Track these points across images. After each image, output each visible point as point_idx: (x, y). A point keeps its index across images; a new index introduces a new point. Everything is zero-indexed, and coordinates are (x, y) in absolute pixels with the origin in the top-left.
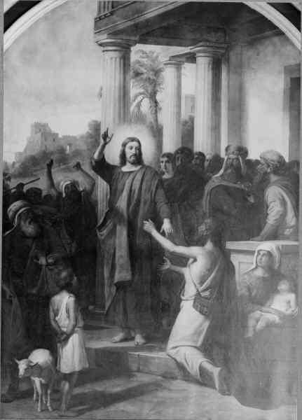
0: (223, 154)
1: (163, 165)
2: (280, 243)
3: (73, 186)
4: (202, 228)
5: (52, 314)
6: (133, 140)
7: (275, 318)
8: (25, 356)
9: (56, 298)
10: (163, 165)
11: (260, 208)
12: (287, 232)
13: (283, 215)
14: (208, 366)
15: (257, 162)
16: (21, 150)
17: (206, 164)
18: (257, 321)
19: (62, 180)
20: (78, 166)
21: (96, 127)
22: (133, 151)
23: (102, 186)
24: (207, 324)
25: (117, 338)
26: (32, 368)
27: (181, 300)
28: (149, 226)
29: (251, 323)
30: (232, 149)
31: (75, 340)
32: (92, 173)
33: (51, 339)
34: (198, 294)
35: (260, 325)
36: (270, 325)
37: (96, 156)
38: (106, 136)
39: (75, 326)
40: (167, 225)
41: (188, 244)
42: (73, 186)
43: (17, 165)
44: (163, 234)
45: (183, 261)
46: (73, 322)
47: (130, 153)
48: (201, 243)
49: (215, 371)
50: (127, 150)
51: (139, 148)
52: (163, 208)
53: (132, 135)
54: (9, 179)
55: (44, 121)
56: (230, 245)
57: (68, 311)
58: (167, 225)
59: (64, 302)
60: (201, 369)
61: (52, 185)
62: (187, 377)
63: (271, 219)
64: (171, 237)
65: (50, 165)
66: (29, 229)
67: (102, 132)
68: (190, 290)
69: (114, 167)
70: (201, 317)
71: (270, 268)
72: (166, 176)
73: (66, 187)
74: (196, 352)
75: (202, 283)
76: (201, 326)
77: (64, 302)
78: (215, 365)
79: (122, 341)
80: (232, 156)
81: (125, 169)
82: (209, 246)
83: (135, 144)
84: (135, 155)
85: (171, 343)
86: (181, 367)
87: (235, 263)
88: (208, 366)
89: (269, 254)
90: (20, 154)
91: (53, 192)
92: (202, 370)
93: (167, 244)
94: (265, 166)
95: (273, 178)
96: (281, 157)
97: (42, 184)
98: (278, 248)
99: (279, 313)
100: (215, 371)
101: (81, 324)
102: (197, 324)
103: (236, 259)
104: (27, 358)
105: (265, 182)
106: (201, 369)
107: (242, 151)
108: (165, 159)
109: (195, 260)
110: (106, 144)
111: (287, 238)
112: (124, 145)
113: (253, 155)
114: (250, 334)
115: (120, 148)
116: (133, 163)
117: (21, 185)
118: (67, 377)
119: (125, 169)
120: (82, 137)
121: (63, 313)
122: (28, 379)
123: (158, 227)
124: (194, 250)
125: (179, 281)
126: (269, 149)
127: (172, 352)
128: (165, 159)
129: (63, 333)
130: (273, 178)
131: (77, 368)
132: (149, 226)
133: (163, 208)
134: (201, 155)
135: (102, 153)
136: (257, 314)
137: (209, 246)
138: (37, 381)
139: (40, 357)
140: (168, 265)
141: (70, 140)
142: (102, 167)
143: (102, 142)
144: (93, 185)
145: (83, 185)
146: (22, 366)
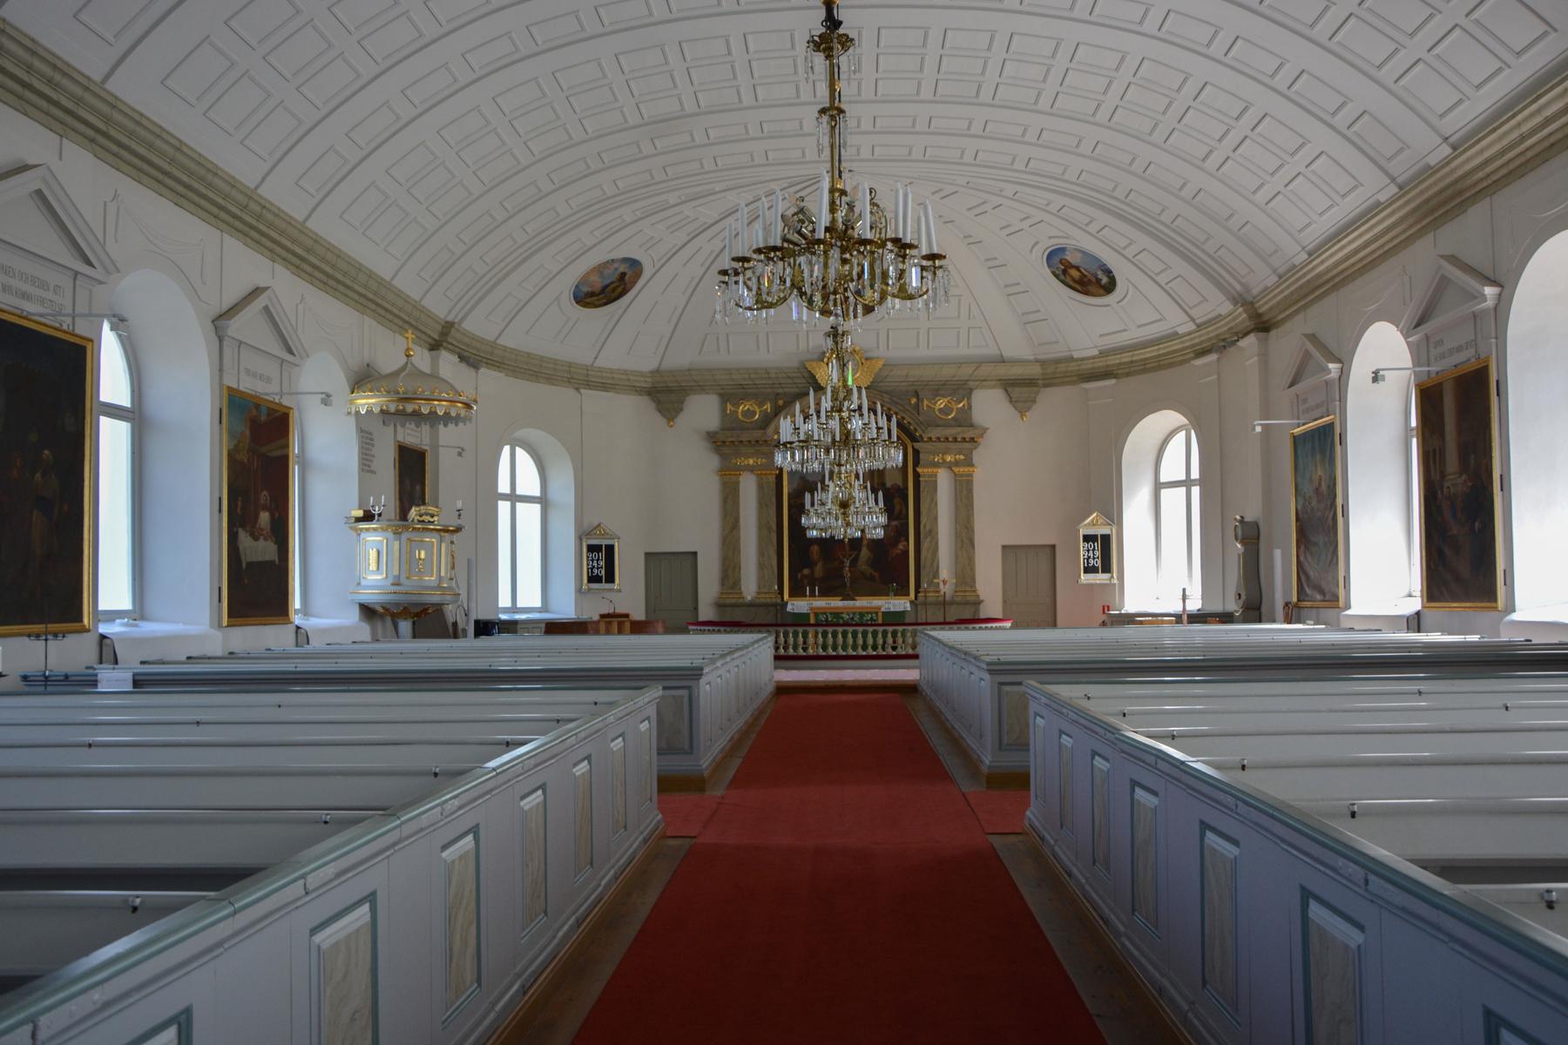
33: (811, 565)
139: (806, 571)
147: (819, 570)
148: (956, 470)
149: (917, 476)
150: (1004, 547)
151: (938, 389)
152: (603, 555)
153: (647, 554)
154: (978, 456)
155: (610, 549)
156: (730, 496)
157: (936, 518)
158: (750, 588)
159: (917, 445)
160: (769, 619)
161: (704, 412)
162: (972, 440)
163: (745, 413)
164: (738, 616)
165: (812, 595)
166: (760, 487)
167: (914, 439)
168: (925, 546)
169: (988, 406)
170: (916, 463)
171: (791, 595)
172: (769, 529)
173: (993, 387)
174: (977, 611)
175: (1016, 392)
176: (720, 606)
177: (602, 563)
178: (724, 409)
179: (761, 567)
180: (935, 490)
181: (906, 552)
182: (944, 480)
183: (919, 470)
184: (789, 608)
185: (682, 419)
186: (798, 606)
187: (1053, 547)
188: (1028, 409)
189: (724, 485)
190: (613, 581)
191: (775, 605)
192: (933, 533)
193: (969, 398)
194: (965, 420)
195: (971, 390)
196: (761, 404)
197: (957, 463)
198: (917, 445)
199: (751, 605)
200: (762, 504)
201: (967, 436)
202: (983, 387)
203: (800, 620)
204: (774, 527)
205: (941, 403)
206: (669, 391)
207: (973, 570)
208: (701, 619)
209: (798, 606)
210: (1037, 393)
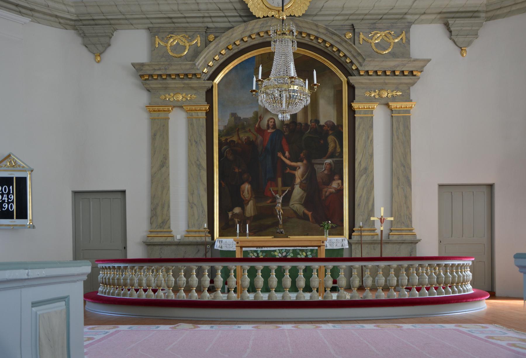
0: (309, 123)
1: (284, 129)
2: (335, 159)
3: (248, 138)
4: (302, 155)
5: (241, 193)
6: (272, 118)
7: (333, 190)
8: (231, 209)
9: (243, 186)
10: (284, 129)
11: (326, 145)
12: (337, 155)
13: (336, 147)
14: (306, 212)
15: (323, 126)
16: (226, 124)
17: (303, 127)
18: (326, 192)
19: (244, 136)
20: (250, 130)
21: (256, 113)
22: (272, 123)
23: (260, 138)
24: (305, 195)
25: (269, 202)
26: (234, 215)
27: (294, 185)
28: (280, 155)
29: (324, 193)
30: (313, 121)
31: (251, 203)
32: (255, 133)
33: (242, 204)
34: (301, 182)
35: (327, 194)
36: (331, 193)
37: (257, 126)
38: (260, 117)
39: (251, 197)
40: (287, 154)
41: (296, 162)
42: (248, 138)
43: (225, 131)
44: (286, 157)
45: (295, 168)
46: (250, 195)
47: (271, 124)
48: (302, 161)
49: (310, 214)
50: (270, 123)
51: (274, 122)
52: (286, 147)
53: (271, 117)
54: (222, 137)
55: (235, 112)
56: (314, 161)
57: (248, 191)
58: (287, 154)
59: (246, 187)
60: (304, 213)
61: (239, 139)
62: (298, 216)
63: (330, 150)
64: (289, 159)
65: (238, 131)
66: (231, 157)
67: (259, 115)
68: (298, 180)
69: (264, 131)
70: (303, 192)
71: (331, 170)
72: (286, 133)
73: (245, 139)
74: (301, 206)
75: (302, 177)
76: (303, 195)
77: (246, 187)
78: (310, 211)
79: (271, 202)
80: (313, 124)
81: (269, 131)
82: (305, 162)
83: (272, 120)
84: (273, 125)
85: (291, 203)
86: (295, 212)
87: (316, 169)
88: (306, 212)
89: (330, 164)
90: (226, 126)
91: (240, 142)
92: (304, 213)
93: (288, 162)
94: (327, 128)
95: (330, 132)
96: (333, 123)
97: (235, 138)
98: (333, 161)
99: (335, 188)
100: (310, 214)
101: (254, 196)
102: (301, 194)
103: (316, 167)
104: (232, 211)
105: (327, 135)
106: (304, 212)
107: (317, 121)
108: (285, 126)
109: (300, 168)
110: (260, 121)
111: (337, 157)
112: (268, 121)
113: (322, 123)
114: (324, 198)
115: (266, 122)
116: (272, 128)
117: (227, 139)
118: (248, 218)
119: (269, 131)
120: (251, 118)
121: (246, 192)
122: (232, 219)
123: (284, 154)
124: (299, 164)
125: (293, 177)
126: (329, 120)
127: (291, 206)
128: (285, 126)
129: (246, 200)
130: (330, 132)
131: (253, 215)
132: (280, 155)
133: (286, 147)
134: (300, 124)
135: (259, 125)
136: (325, 189)
137: (305, 162)
138: (236, 220)
139: (237, 210)
140: (288, 171)
141: (246, 119)
142: (260, 131)
143: (259, 120)
144: (256, 139)
145: (252, 137)
146: (230, 214)
147: (250, 209)
148: (393, 105)
149: (352, 111)
150: (441, 186)
151: (376, 22)
152: (13, 188)
153: (76, 193)
154: (415, 92)
155: (22, 182)
156: (159, 134)
157: (372, 156)
158: (179, 227)
159: (353, 80)
160: (200, 255)
161: (132, 46)
162: (411, 73)
163: (175, 48)
164: (167, 253)
165: (243, 233)
166: (190, 123)
167: (348, 73)
168: (359, 184)
169: (427, 41)
170: (352, 98)
171: (221, 235)
172: (199, 166)
173: (432, 22)
174: (414, 249)
175: (456, 25)
176: (149, 244)
177: (13, 197)
178: (152, 44)
179: (191, 205)
180: (371, 127)
181: (340, 191)
182: (380, 118)
183: (355, 105)
184: (217, 246)
185: (110, 54)
186: (226, 244)
187: (491, 186)
188: (469, 44)
189: (153, 121)
190: (25, 217)
191: (204, 244)
192: (368, 171)
193: (408, 32)
194: (403, 51)
195: (410, 24)
196: (192, 38)
197: (394, 99)
198: (353, 80)
199: (179, 244)
200: (191, 142)
201: (406, 70)
202: (422, 22)
203: (228, 257)
204: (204, 164)
205: (378, 38)
206: (94, 22)
207: (409, 208)
208: (130, 256)
209: (226, 244)
210: (481, 25)
